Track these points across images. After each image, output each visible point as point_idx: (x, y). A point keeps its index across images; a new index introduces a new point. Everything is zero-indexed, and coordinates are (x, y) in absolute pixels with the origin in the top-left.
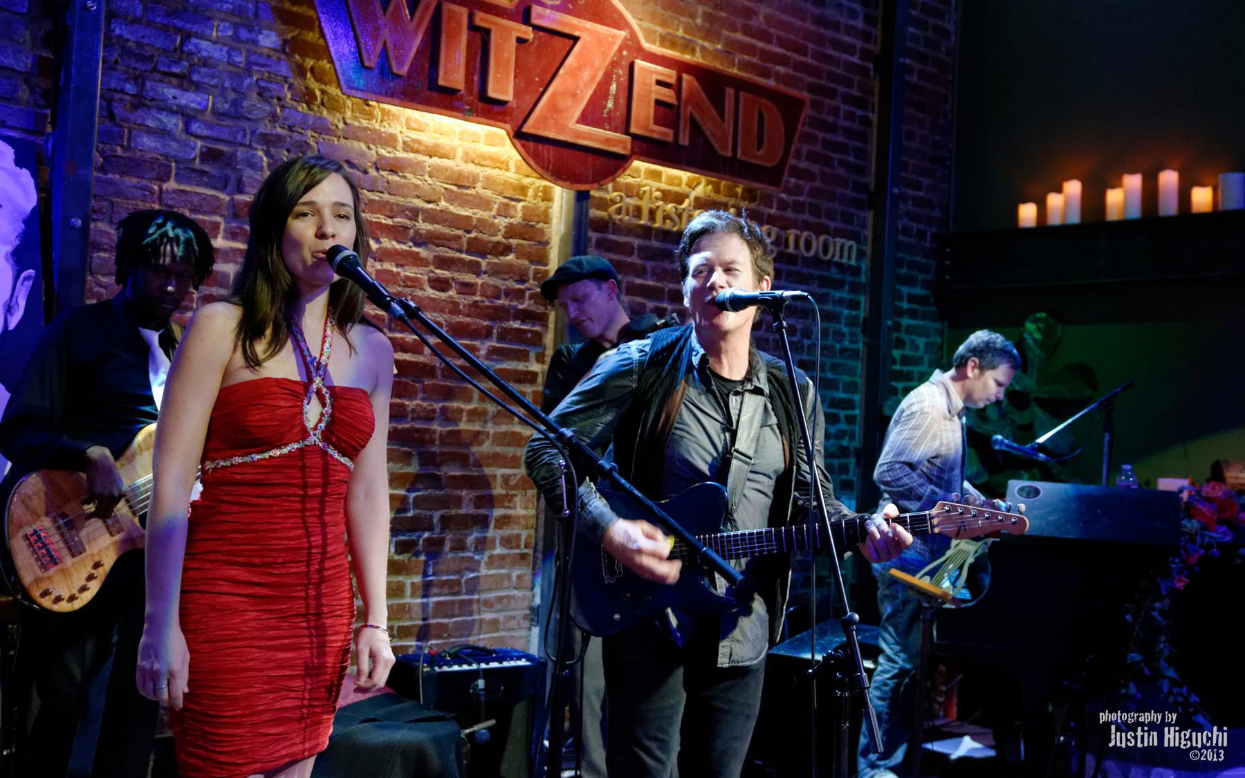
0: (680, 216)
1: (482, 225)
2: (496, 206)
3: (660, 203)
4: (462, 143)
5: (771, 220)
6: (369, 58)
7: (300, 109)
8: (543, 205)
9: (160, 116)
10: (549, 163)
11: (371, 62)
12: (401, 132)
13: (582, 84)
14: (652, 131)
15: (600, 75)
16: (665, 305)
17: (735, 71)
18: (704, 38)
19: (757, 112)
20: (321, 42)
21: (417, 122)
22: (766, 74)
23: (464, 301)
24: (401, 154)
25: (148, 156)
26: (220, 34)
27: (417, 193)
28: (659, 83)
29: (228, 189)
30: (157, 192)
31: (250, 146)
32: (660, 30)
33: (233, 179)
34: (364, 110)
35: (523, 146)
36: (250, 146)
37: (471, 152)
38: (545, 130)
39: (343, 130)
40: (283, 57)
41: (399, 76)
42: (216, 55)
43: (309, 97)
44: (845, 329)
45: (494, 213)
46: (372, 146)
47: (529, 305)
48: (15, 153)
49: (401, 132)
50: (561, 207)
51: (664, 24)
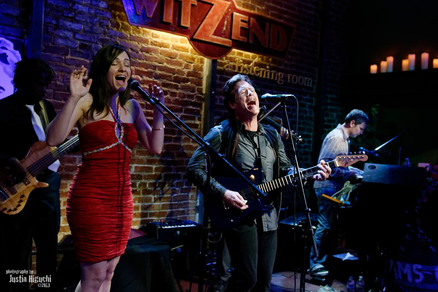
0: (249, 69)
1: (179, 72)
2: (184, 65)
3: (242, 64)
4: (172, 42)
5: (282, 71)
6: (138, 12)
7: (114, 30)
8: (200, 65)
9: (65, 32)
11: (139, 12)
12: (150, 38)
13: (214, 21)
14: (239, 38)
15: (221, 18)
17: (269, 17)
18: (258, 5)
20: (121, 6)
21: (156, 35)
22: (280, 18)
23: (172, 99)
24: (150, 46)
25: (61, 46)
26: (86, 3)
27: (156, 60)
28: (242, 21)
31: (97, 43)
33: (91, 55)
34: (137, 30)
35: (194, 43)
36: (97, 43)
37: (175, 45)
38: (201, 37)
39: (130, 37)
40: (108, 11)
42: (84, 10)
43: (117, 26)
44: (308, 110)
45: (183, 67)
46: (140, 43)
47: (195, 100)
48: (14, 45)
50: (207, 65)
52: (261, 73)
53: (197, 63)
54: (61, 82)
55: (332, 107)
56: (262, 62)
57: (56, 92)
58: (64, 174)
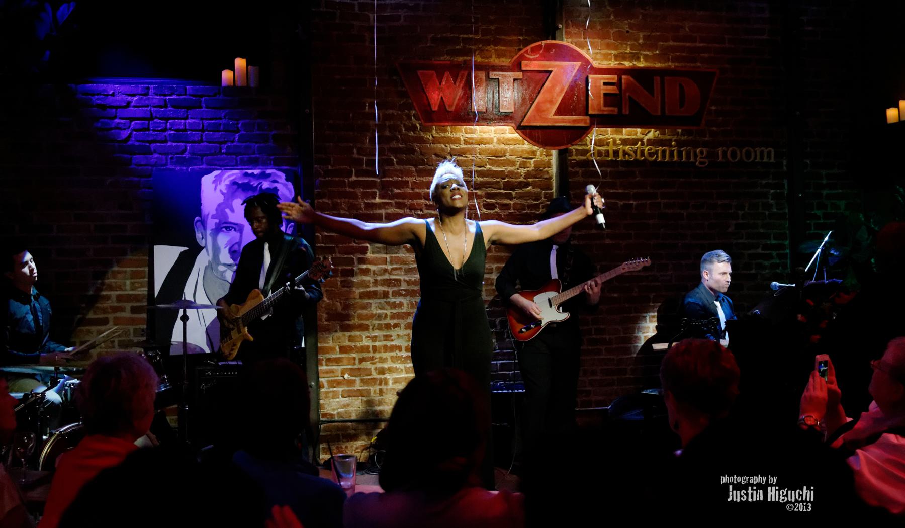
1: (511, 174)
2: (518, 163)
4: (495, 135)
5: (705, 144)
7: (410, 134)
8: (546, 159)
10: (539, 138)
12: (462, 136)
13: (555, 95)
14: (604, 111)
16: (632, 202)
21: (471, 129)
24: (463, 146)
30: (347, 183)
32: (614, 52)
35: (523, 133)
37: (502, 139)
39: (432, 140)
41: (451, 112)
45: (518, 167)
46: (447, 145)
48: (286, 176)
49: (462, 136)
51: (616, 48)
53: (541, 158)
54: (345, 210)
55: (828, 192)
58: (357, 324)
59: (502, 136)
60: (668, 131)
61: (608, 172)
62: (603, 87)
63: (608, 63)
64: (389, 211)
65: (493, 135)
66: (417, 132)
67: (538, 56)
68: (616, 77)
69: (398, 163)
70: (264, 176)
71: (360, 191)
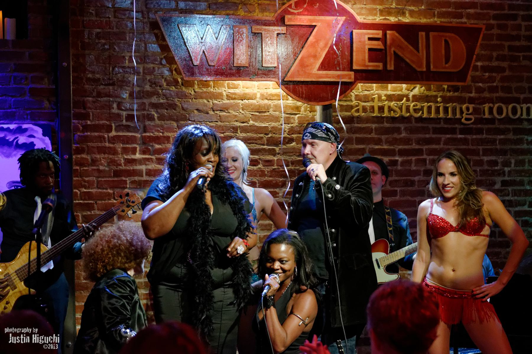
0: (401, 108)
4: (259, 90)
5: (471, 101)
8: (310, 115)
10: (303, 93)
12: (225, 91)
13: (319, 50)
16: (397, 158)
19: (443, 41)
21: (233, 84)
23: (267, 169)
27: (236, 119)
29: (140, 132)
30: (107, 138)
32: (379, 7)
35: (286, 88)
37: (265, 94)
46: (209, 100)
48: (43, 131)
49: (225, 91)
52: (425, 109)
53: (305, 113)
54: (104, 166)
56: (427, 93)
57: (100, 179)
59: (266, 91)
60: (433, 86)
61: (373, 128)
62: (367, 42)
63: (374, 18)
64: (150, 167)
65: (256, 91)
66: (179, 87)
67: (301, 10)
68: (380, 32)
69: (160, 118)
70: (20, 131)
71: (119, 147)
